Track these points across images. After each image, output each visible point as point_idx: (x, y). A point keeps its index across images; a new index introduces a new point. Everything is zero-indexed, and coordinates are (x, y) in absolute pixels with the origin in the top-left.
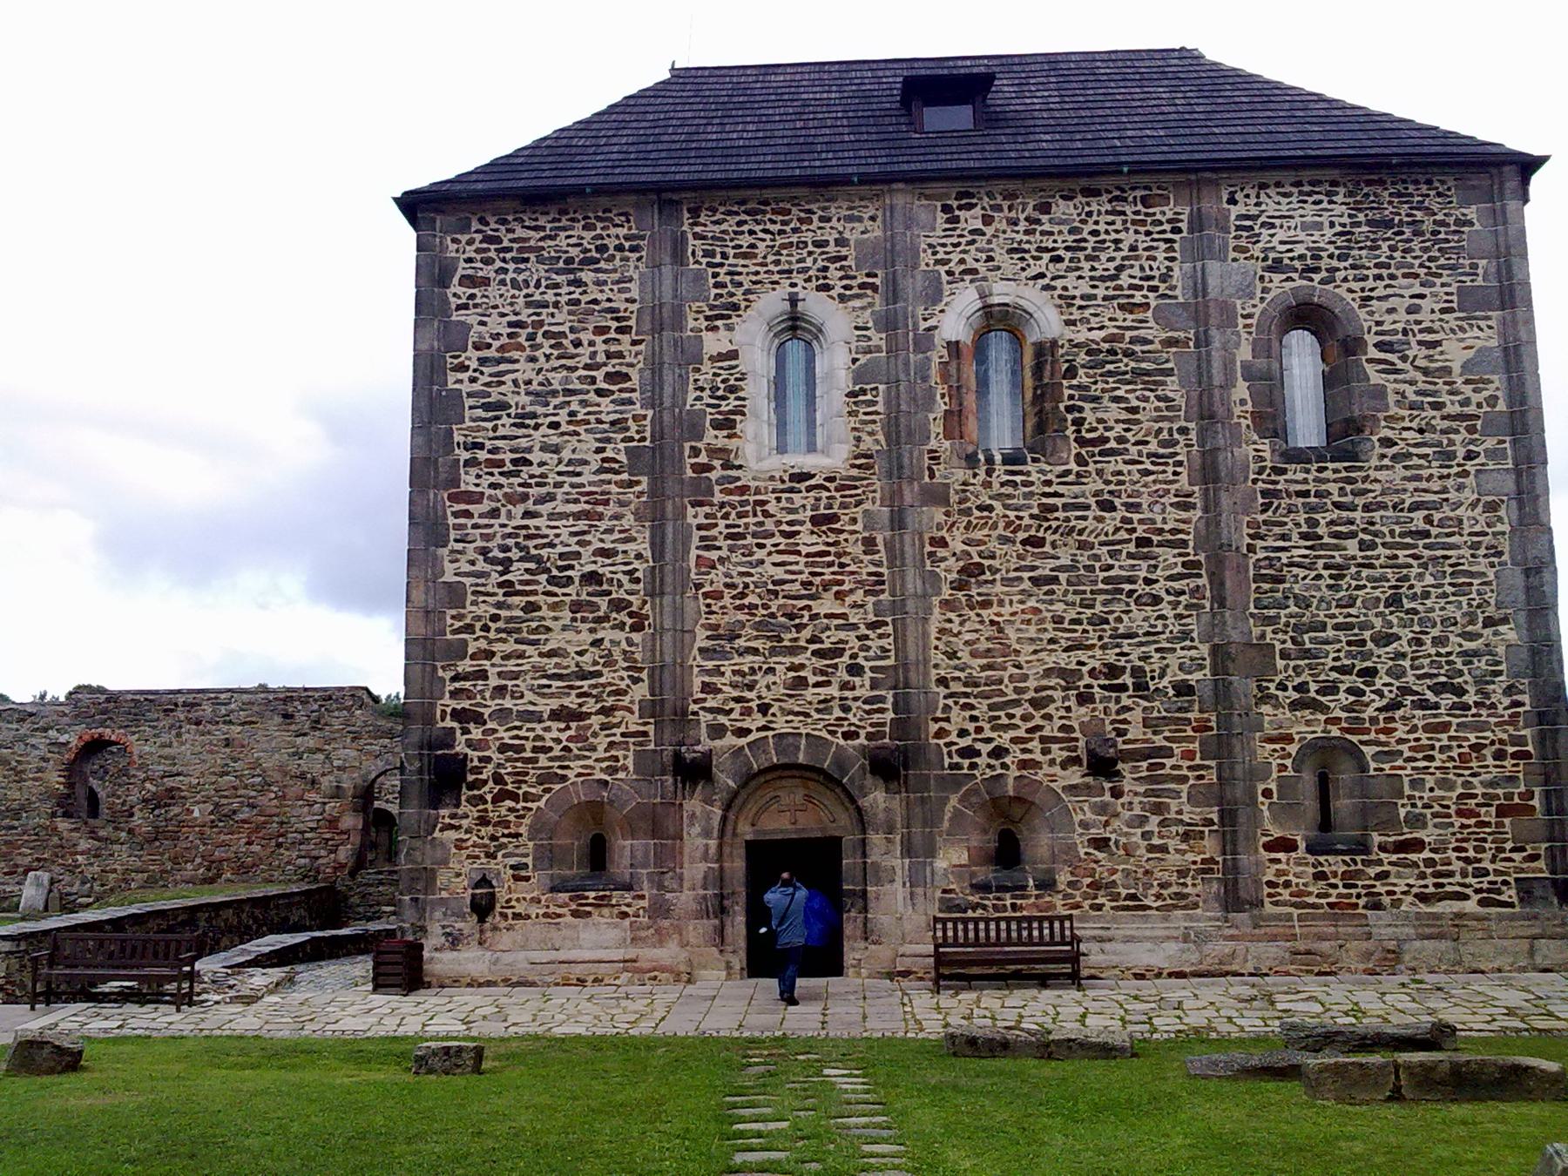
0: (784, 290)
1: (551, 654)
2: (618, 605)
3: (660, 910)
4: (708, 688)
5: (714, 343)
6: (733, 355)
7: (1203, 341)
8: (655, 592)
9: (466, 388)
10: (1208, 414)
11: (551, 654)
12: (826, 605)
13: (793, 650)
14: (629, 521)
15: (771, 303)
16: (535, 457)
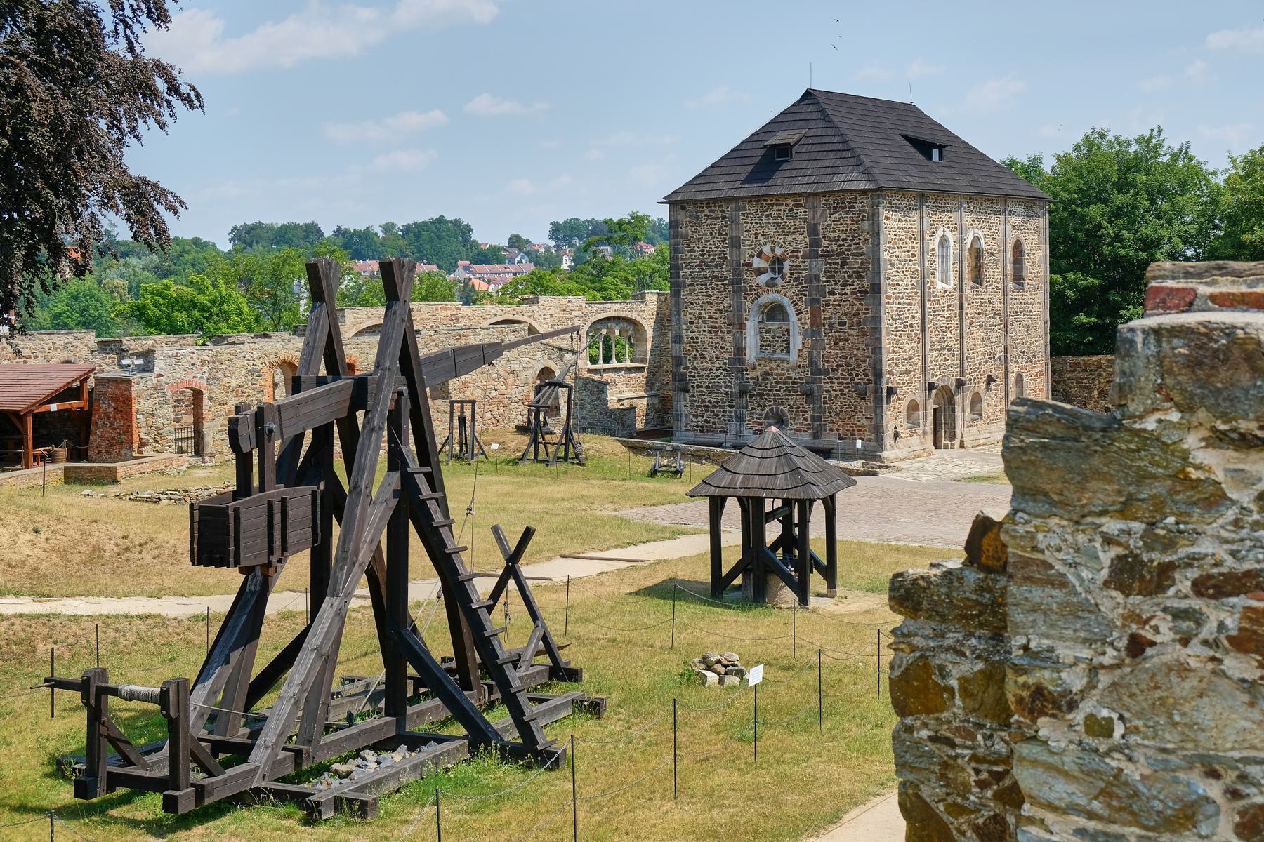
0: (941, 229)
1: (905, 352)
2: (916, 334)
3: (925, 433)
4: (931, 362)
5: (931, 247)
6: (934, 250)
7: (1005, 251)
8: (924, 330)
9: (888, 258)
10: (1005, 275)
11: (905, 352)
12: (949, 335)
13: (944, 349)
14: (917, 306)
15: (940, 233)
16: (900, 283)
